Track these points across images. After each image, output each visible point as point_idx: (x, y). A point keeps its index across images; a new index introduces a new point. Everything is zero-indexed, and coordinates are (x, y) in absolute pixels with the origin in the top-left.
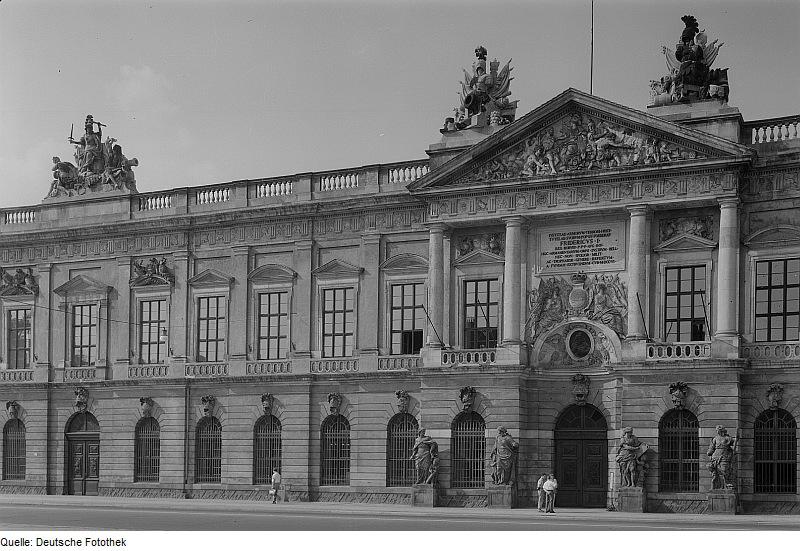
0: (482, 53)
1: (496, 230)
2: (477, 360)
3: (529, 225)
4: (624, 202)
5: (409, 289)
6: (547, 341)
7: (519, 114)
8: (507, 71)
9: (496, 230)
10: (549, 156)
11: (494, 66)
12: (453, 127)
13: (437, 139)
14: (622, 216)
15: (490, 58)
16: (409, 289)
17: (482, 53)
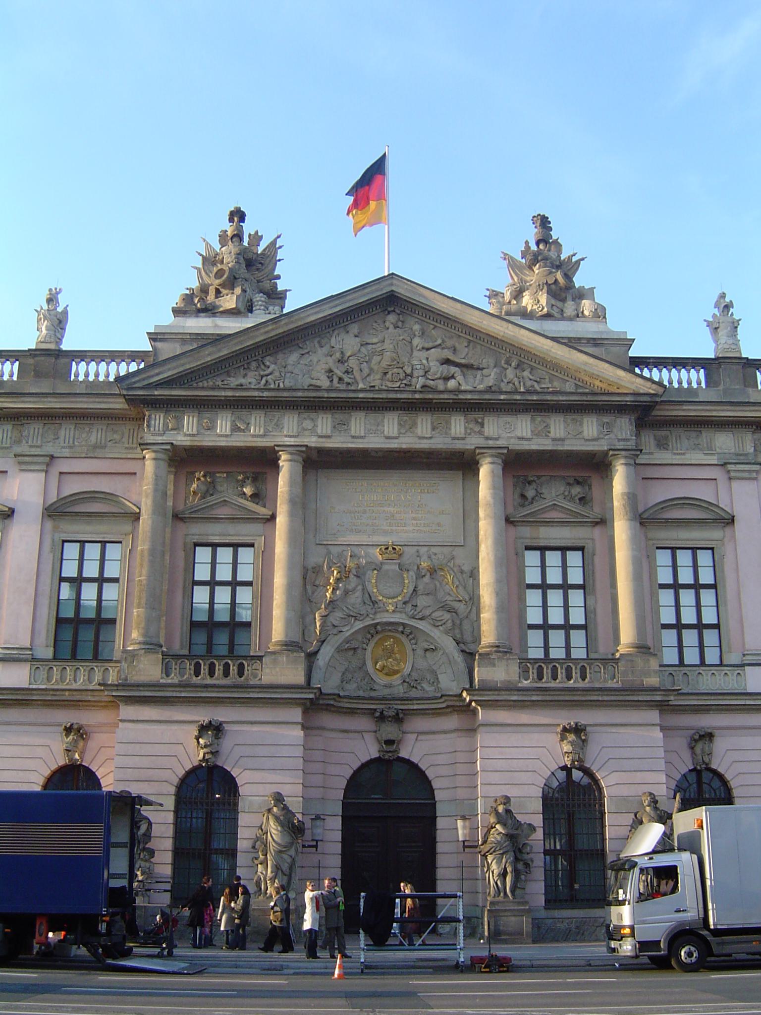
0: (238, 216)
1: (262, 462)
2: (226, 674)
3: (317, 462)
4: (472, 443)
5: (92, 551)
6: (339, 650)
7: (290, 305)
8: (273, 246)
9: (262, 462)
10: (353, 363)
11: (256, 238)
12: (193, 304)
13: (167, 319)
14: (464, 464)
15: (248, 228)
16: (92, 551)
17: (238, 216)
